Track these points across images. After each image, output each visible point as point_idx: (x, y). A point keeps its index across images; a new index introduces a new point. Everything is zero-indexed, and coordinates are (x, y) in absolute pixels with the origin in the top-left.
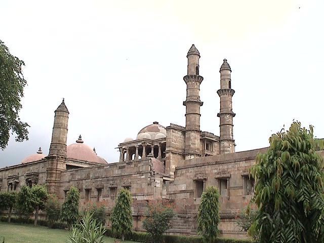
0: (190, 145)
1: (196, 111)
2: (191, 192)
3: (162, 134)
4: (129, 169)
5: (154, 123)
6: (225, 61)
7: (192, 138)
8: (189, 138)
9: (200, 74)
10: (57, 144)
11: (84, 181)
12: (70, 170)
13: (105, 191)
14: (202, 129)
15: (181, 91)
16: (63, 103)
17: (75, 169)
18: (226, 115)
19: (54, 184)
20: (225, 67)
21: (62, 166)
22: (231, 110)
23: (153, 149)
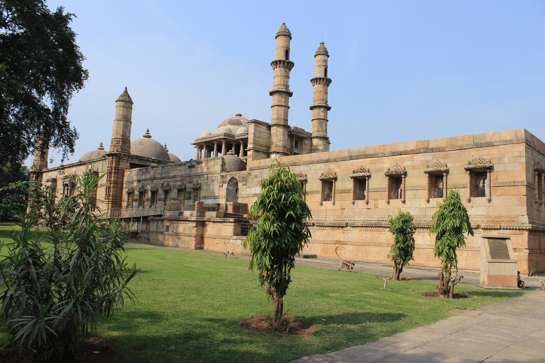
13: (174, 194)
16: (126, 92)
23: (234, 145)
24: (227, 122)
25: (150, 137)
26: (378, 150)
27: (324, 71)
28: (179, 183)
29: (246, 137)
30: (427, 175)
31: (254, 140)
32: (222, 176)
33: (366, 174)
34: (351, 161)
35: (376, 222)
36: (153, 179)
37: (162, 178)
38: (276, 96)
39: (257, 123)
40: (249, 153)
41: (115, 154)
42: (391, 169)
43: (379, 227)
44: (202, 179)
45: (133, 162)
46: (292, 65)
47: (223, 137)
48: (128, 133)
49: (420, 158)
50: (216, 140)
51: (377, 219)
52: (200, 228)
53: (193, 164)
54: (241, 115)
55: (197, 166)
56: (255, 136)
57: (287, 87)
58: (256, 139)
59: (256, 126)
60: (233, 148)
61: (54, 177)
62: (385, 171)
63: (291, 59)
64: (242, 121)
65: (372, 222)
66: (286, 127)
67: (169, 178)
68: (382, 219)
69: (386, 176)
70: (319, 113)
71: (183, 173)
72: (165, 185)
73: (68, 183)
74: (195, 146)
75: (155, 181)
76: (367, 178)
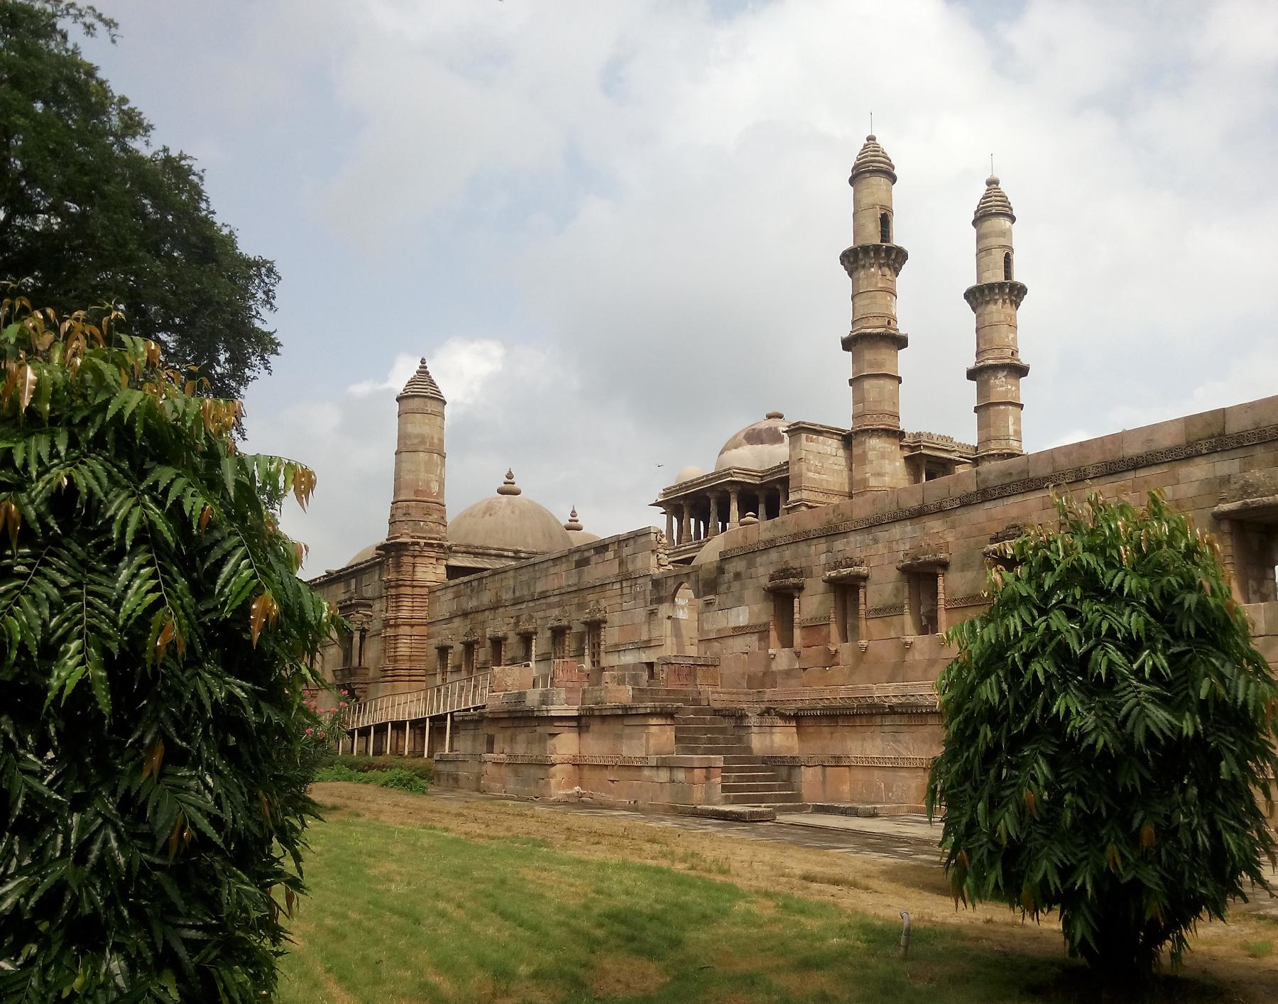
1: (881, 365)
2: (761, 632)
3: (778, 453)
4: (600, 566)
5: (769, 417)
6: (992, 183)
8: (863, 459)
10: (414, 503)
11: (487, 613)
14: (908, 424)
15: (834, 305)
17: (466, 579)
18: (995, 371)
19: (407, 630)
20: (993, 210)
21: (431, 572)
23: (762, 499)
24: (741, 437)
26: (1063, 462)
30: (1225, 527)
34: (988, 505)
44: (608, 593)
49: (1199, 471)
53: (586, 554)
54: (780, 416)
55: (594, 559)
58: (811, 474)
63: (897, 240)
71: (564, 583)
75: (501, 610)
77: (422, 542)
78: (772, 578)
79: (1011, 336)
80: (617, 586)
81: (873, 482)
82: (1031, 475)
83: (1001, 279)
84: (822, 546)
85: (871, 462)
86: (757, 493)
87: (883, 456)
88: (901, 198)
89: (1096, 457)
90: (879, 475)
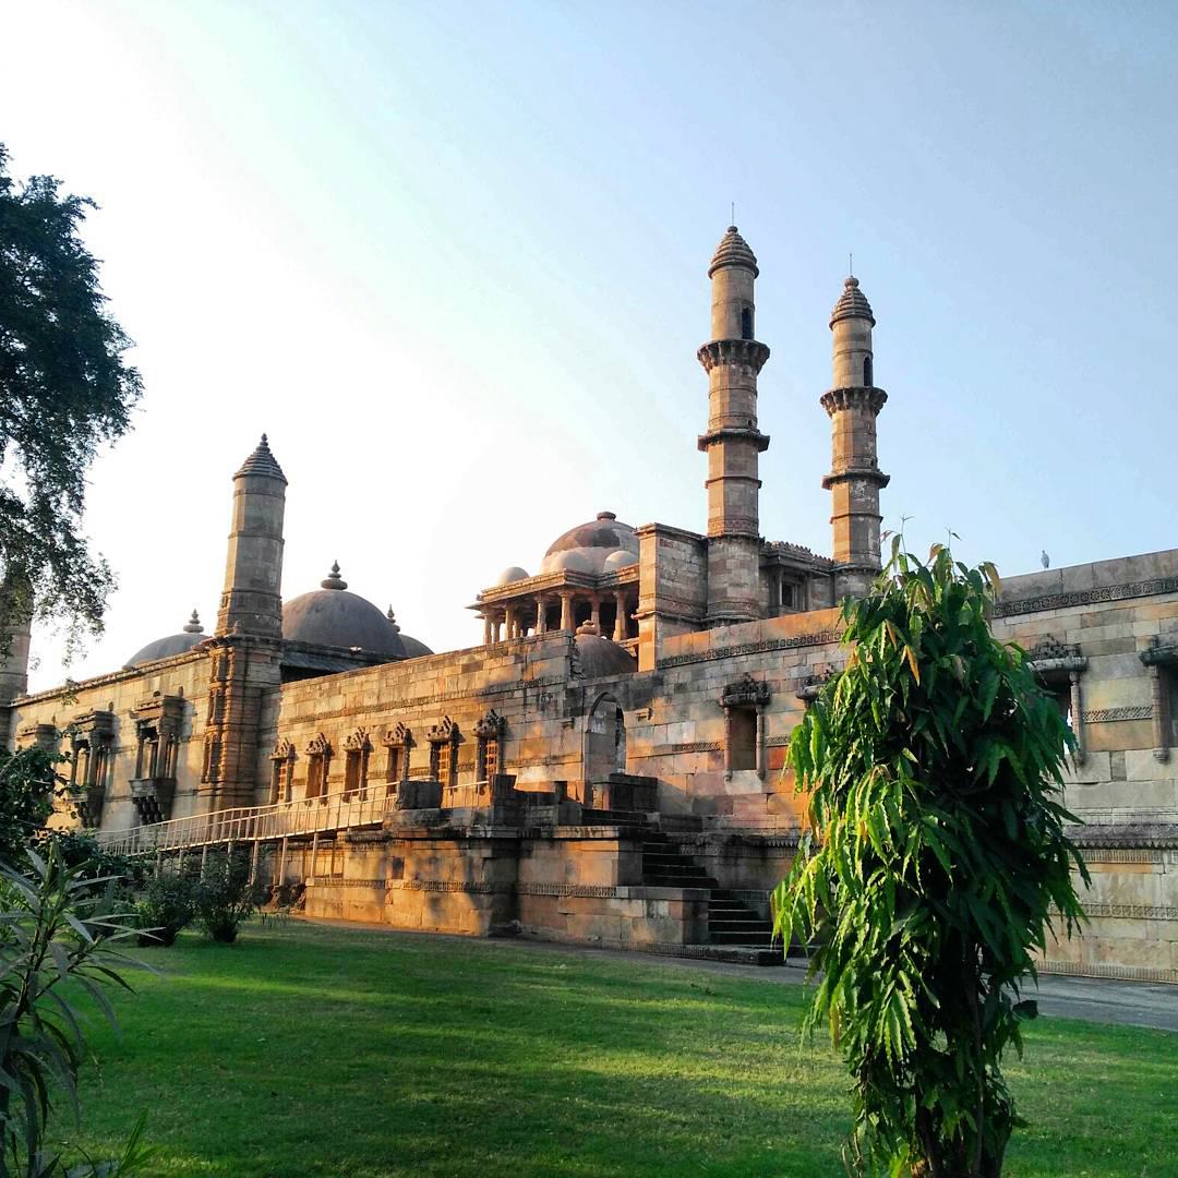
0: (725, 590)
7: (730, 563)
8: (721, 567)
9: (759, 337)
12: (293, 684)
16: (264, 449)
20: (856, 311)
22: (874, 462)
25: (344, 586)
26: (1106, 578)
27: (861, 368)
28: (435, 721)
29: (632, 578)
31: (658, 585)
32: (571, 693)
33: (1066, 661)
34: (1010, 620)
35: (1122, 830)
36: (352, 712)
37: (380, 708)
38: (720, 448)
39: (664, 533)
40: (645, 626)
41: (233, 639)
42: (1166, 638)
43: (1138, 847)
45: (287, 663)
46: (763, 352)
47: (563, 582)
48: (272, 575)
50: (543, 592)
51: (1130, 820)
52: (507, 863)
53: (477, 657)
54: (611, 516)
56: (660, 575)
57: (751, 420)
58: (664, 581)
59: (661, 545)
60: (595, 616)
61: (45, 720)
62: (1142, 647)
63: (759, 337)
64: (617, 532)
65: (1107, 830)
66: (754, 541)
67: (404, 704)
68: (1144, 820)
69: (1147, 664)
70: (852, 497)
72: (392, 727)
73: (86, 736)
74: (479, 613)
76: (1072, 677)
77: (257, 638)
78: (728, 691)
79: (871, 444)
80: (519, 694)
81: (731, 593)
82: (1066, 590)
83: (861, 384)
84: (793, 656)
85: (729, 571)
86: (591, 599)
87: (743, 565)
88: (764, 293)
89: (1148, 574)
90: (738, 585)
